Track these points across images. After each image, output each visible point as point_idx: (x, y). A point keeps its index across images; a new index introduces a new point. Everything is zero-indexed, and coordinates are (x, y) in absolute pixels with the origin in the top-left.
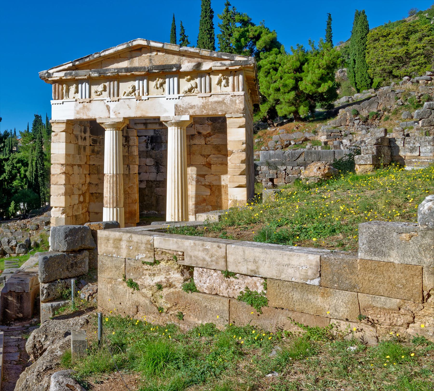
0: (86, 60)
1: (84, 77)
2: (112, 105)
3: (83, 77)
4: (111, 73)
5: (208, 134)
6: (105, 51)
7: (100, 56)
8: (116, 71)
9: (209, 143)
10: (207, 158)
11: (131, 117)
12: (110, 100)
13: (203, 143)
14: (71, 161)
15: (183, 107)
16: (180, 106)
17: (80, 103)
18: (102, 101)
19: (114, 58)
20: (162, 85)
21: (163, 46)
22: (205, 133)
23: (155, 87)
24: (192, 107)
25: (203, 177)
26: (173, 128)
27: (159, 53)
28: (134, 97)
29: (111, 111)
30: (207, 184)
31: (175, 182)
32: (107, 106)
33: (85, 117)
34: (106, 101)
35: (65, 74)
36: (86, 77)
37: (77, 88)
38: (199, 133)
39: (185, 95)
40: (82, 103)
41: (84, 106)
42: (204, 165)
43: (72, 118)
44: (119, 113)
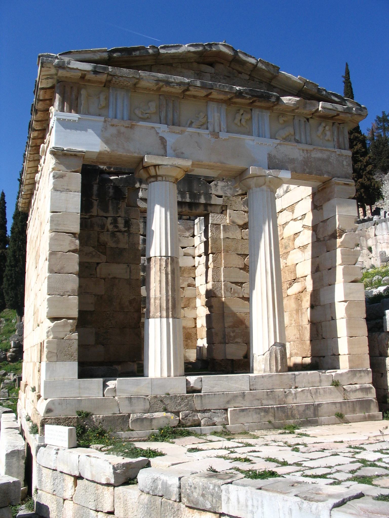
0: (134, 53)
2: (171, 140)
6: (168, 47)
7: (159, 53)
8: (187, 80)
9: (246, 237)
13: (239, 238)
16: (275, 157)
19: (171, 65)
20: (247, 121)
21: (258, 62)
22: (241, 223)
23: (239, 124)
24: (292, 161)
25: (240, 286)
27: (240, 75)
28: (207, 132)
29: (168, 148)
35: (95, 67)
37: (107, 99)
38: (233, 222)
40: (116, 126)
41: (119, 133)
42: (241, 269)
44: (182, 153)
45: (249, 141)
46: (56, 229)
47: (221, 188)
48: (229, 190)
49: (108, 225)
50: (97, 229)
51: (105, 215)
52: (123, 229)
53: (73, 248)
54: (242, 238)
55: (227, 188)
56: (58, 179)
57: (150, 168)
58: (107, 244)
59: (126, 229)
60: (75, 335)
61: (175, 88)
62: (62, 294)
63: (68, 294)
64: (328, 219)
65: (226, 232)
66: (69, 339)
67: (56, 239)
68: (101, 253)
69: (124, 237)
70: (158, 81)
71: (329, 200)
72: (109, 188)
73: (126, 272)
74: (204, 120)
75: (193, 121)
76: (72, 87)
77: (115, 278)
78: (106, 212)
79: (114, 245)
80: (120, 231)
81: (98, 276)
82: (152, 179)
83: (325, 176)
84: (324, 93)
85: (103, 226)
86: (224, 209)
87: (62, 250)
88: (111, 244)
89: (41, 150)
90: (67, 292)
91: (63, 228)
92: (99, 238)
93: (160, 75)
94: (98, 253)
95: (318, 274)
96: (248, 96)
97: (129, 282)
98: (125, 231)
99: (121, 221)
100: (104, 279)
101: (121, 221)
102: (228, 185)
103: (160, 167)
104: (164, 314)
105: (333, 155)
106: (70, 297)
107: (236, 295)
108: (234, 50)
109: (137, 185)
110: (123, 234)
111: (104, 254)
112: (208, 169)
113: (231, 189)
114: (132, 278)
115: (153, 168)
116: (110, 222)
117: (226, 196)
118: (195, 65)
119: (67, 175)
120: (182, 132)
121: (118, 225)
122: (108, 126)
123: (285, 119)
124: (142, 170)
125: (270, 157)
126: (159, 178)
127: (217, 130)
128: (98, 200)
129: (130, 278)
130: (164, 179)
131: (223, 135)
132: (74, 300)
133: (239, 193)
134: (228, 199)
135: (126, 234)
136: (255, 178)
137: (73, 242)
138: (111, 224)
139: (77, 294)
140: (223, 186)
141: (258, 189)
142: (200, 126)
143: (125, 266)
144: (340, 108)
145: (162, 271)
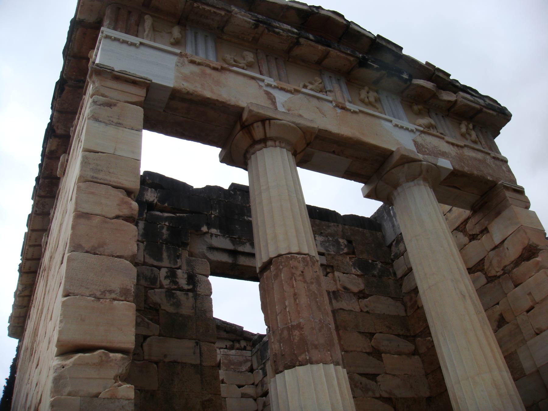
1: (218, 11)
3: (215, 10)
4: (283, 30)
5: (361, 292)
10: (371, 341)
11: (330, 133)
12: (274, 84)
13: (357, 309)
15: (428, 149)
17: (193, 62)
18: (253, 82)
20: (376, 101)
22: (355, 289)
25: (372, 380)
26: (422, 182)
30: (385, 395)
31: (470, 296)
32: (268, 93)
33: (208, 94)
34: (261, 84)
36: (223, 13)
38: (345, 288)
39: (425, 130)
40: (199, 64)
42: (368, 354)
46: (93, 177)
47: (321, 244)
48: (331, 247)
49: (162, 279)
51: (156, 263)
52: (186, 287)
53: (125, 212)
54: (362, 311)
55: (327, 244)
56: (102, 107)
57: (255, 125)
58: (160, 306)
59: (191, 287)
60: (127, 391)
61: (281, 35)
62: (98, 294)
63: (113, 295)
64: (503, 241)
65: (338, 301)
66: (113, 398)
67: (93, 193)
68: (151, 320)
69: (188, 299)
70: (258, 21)
71: (498, 214)
72: (162, 228)
73: (194, 353)
75: (307, 84)
76: (130, 12)
77: (175, 362)
78: (158, 260)
79: (171, 310)
80: (181, 290)
81: (146, 357)
82: (257, 147)
83: (489, 178)
84: (457, 84)
86: (328, 270)
87: (103, 213)
88: (167, 307)
89: (60, 164)
90: (111, 291)
91: (108, 178)
92: (146, 296)
93: (260, 16)
94: (146, 320)
95: (505, 329)
96: (376, 66)
97: (198, 368)
98: (189, 290)
100: (157, 363)
102: (328, 241)
103: (272, 121)
104: (315, 355)
105: (488, 157)
106: (116, 302)
107: (370, 393)
108: (345, 20)
109: (205, 229)
110: (187, 294)
111: (157, 322)
112: (334, 152)
113: (333, 245)
114: (204, 364)
115: (259, 124)
116: (165, 274)
117: (329, 254)
119: (118, 105)
121: (177, 280)
122: (186, 62)
123: (420, 107)
124: (241, 132)
126: (269, 143)
127: (340, 100)
128: (145, 243)
129: (201, 364)
130: (277, 143)
132: (126, 311)
133: (345, 252)
134: (333, 258)
135: (191, 294)
136: (406, 166)
137: (126, 203)
138: (166, 277)
139: (131, 299)
140: (323, 242)
141: (411, 184)
143: (191, 344)
144: (481, 101)
145: (298, 278)
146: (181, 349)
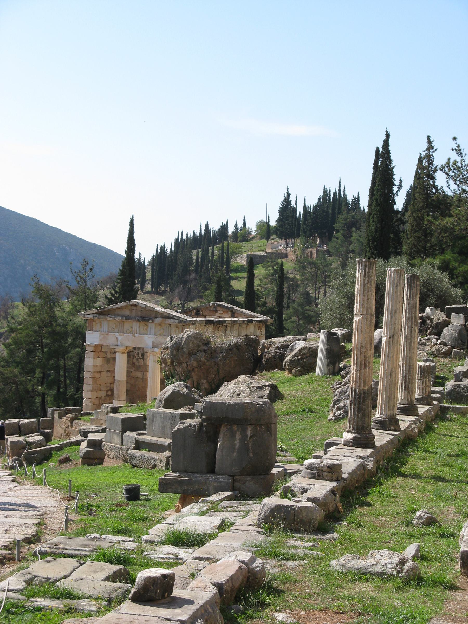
2: (120, 338)
14: (99, 369)
35: (93, 316)
43: (97, 343)
45: (146, 337)
50: (132, 357)
74: (130, 330)
79: (137, 364)
85: (134, 356)
88: (137, 363)
97: (142, 379)
99: (140, 354)
101: (140, 354)
111: (134, 367)
118: (130, 307)
120: (123, 335)
125: (153, 343)
131: (136, 335)
142: (130, 333)
144: (177, 321)
146: (139, 374)
